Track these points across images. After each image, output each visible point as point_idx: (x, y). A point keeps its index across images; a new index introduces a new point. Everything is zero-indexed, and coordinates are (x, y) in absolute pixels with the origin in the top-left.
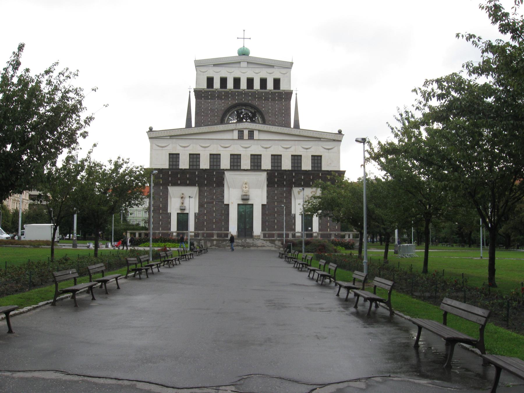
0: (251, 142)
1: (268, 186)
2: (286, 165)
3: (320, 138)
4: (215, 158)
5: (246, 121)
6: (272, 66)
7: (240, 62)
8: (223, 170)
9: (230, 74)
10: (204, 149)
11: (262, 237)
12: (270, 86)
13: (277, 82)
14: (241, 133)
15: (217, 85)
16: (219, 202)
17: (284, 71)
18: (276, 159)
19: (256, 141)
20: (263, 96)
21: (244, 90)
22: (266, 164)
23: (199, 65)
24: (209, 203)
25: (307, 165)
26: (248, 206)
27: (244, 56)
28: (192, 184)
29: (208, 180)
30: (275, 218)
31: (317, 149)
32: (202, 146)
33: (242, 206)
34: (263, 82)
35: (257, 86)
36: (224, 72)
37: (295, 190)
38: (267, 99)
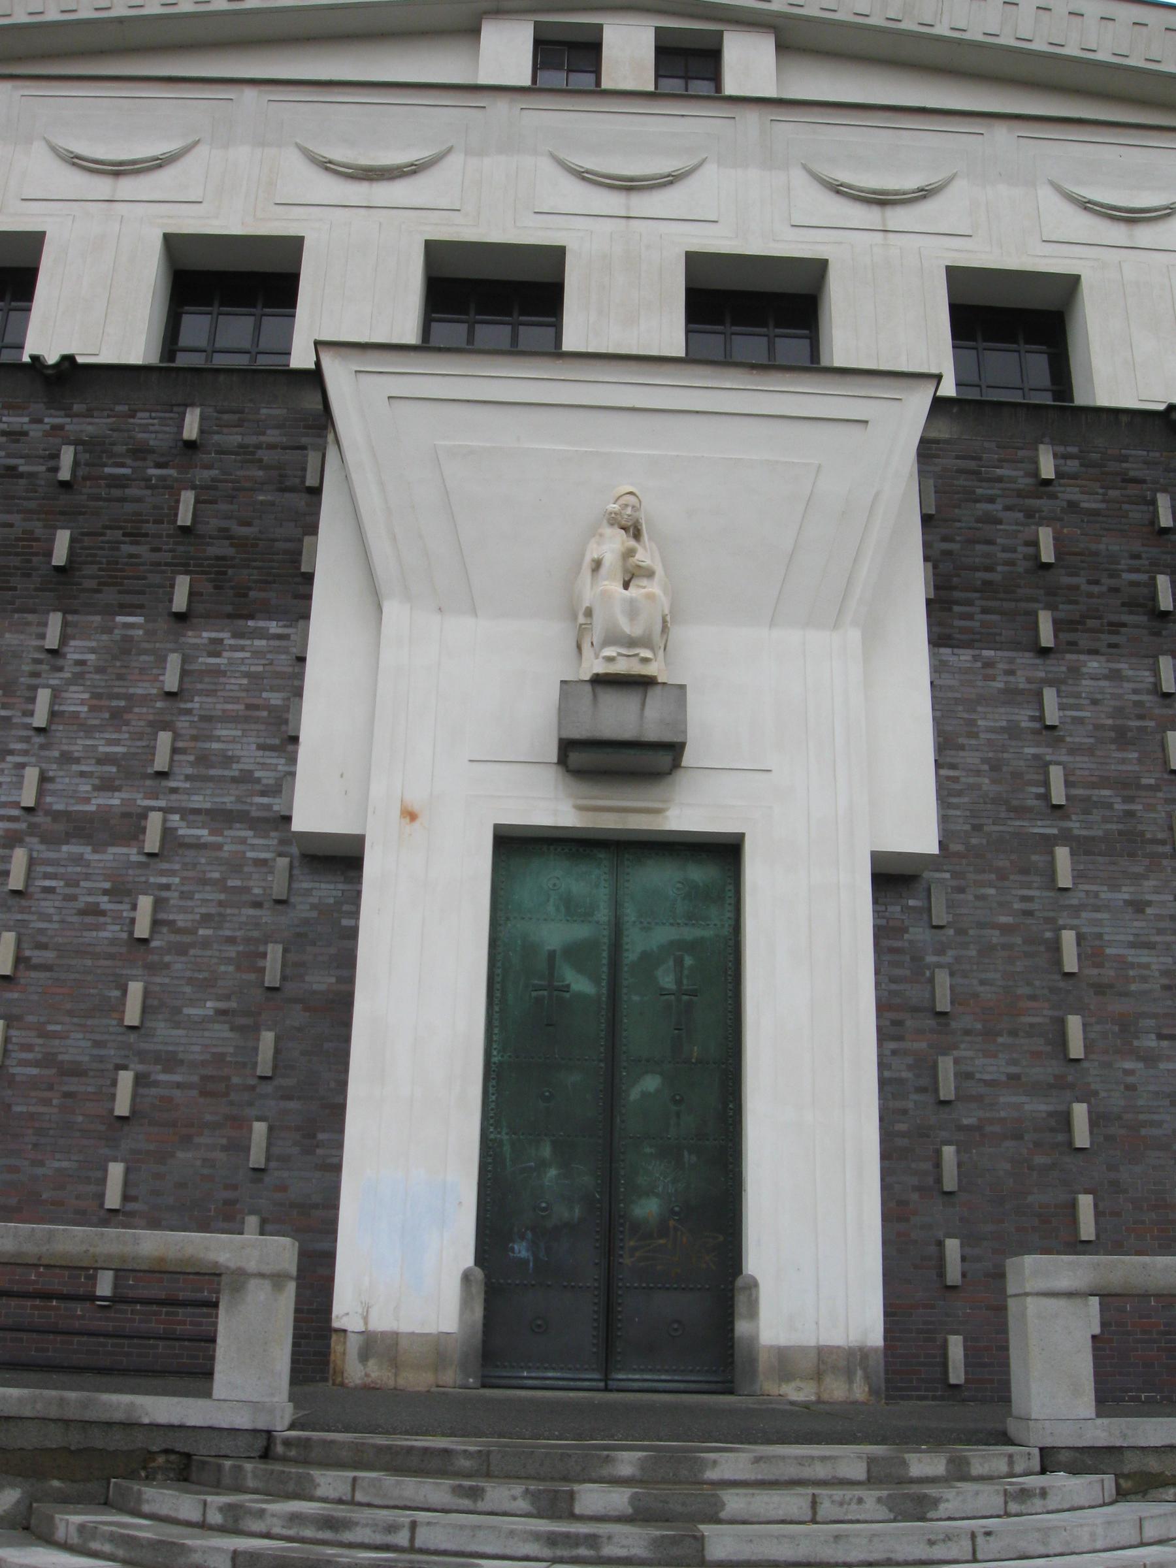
4: (231, 284)
10: (102, 186)
16: (221, 818)
19: (752, 118)
24: (81, 828)
26: (660, 878)
30: (1068, 1080)
32: (76, 161)
33: (555, 877)
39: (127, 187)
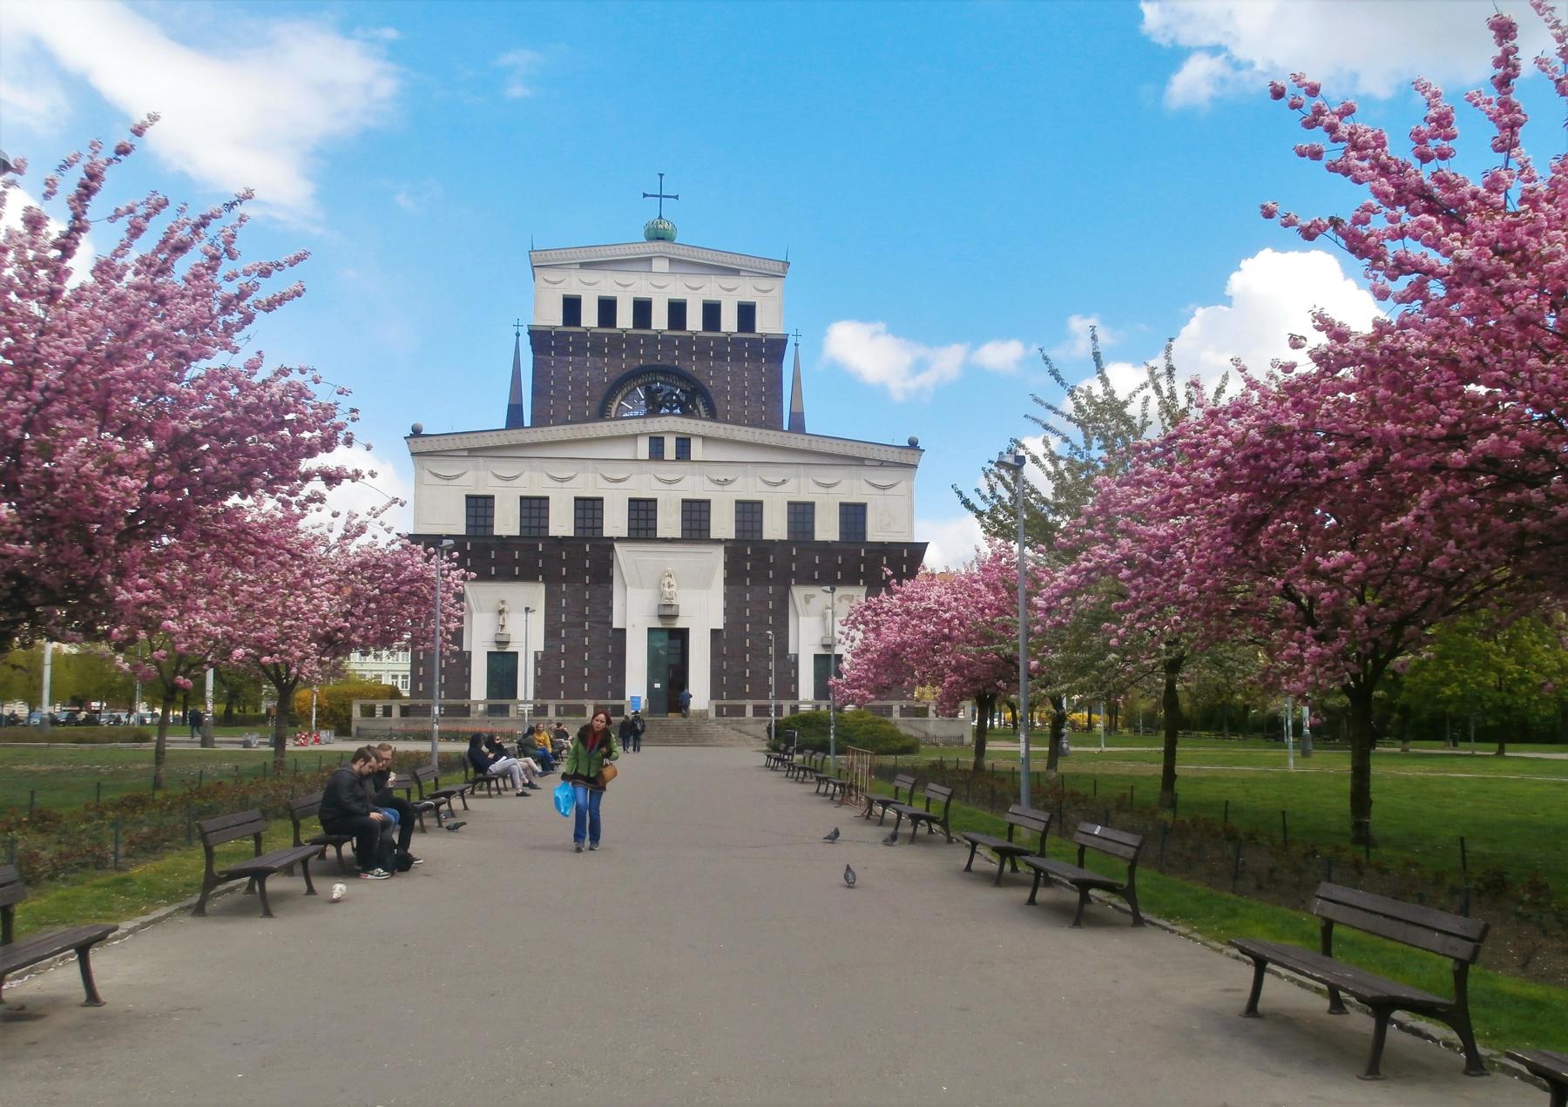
0: (682, 467)
1: (727, 581)
2: (775, 527)
3: (863, 459)
4: (588, 509)
5: (671, 414)
6: (735, 272)
7: (649, 260)
8: (611, 538)
9: (625, 290)
10: (559, 484)
11: (712, 715)
12: (729, 322)
13: (747, 313)
14: (657, 444)
15: (589, 317)
17: (765, 284)
18: (749, 512)
19: (696, 466)
21: (660, 332)
22: (723, 524)
24: (574, 625)
25: (827, 529)
27: (661, 243)
28: (528, 576)
29: (571, 564)
30: (746, 665)
31: (852, 487)
34: (712, 312)
35: (694, 321)
36: (605, 284)
37: (798, 593)
38: (720, 356)
39: (565, 484)
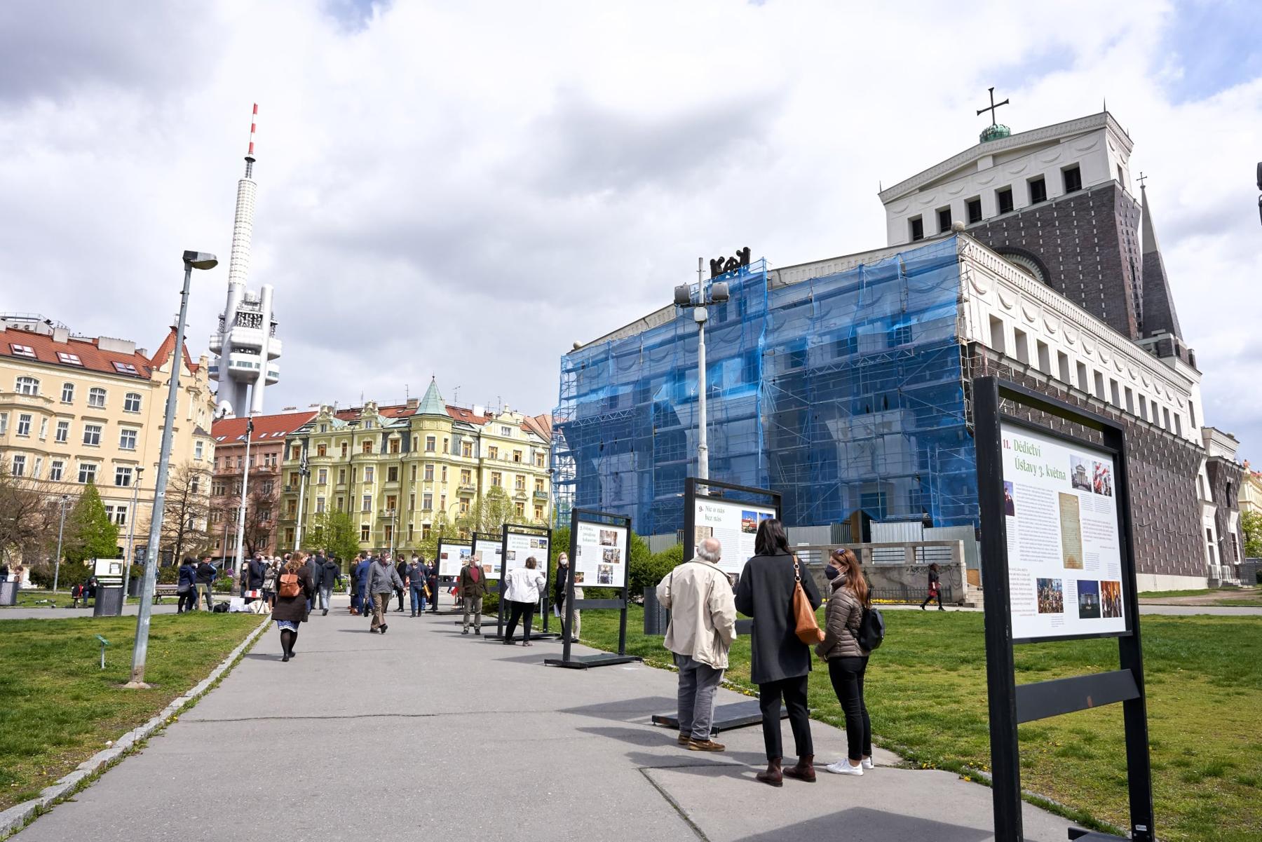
6: (1056, 142)
12: (1055, 189)
13: (1072, 177)
20: (1038, 219)
23: (890, 198)
